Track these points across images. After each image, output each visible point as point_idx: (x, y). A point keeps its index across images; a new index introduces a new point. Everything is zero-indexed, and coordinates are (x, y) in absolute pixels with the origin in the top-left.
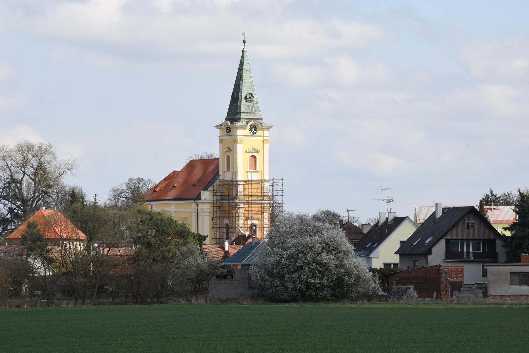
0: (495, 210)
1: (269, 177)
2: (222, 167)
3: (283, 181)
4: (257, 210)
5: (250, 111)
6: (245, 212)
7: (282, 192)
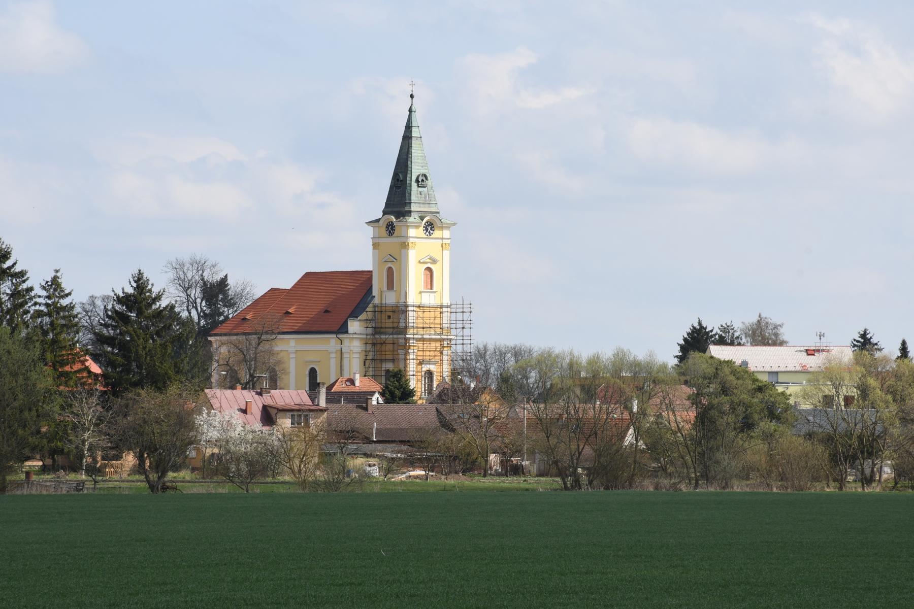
0: (824, 353)
1: (450, 300)
2: (378, 284)
3: (472, 306)
4: (434, 350)
5: (423, 201)
6: (419, 352)
7: (469, 322)
